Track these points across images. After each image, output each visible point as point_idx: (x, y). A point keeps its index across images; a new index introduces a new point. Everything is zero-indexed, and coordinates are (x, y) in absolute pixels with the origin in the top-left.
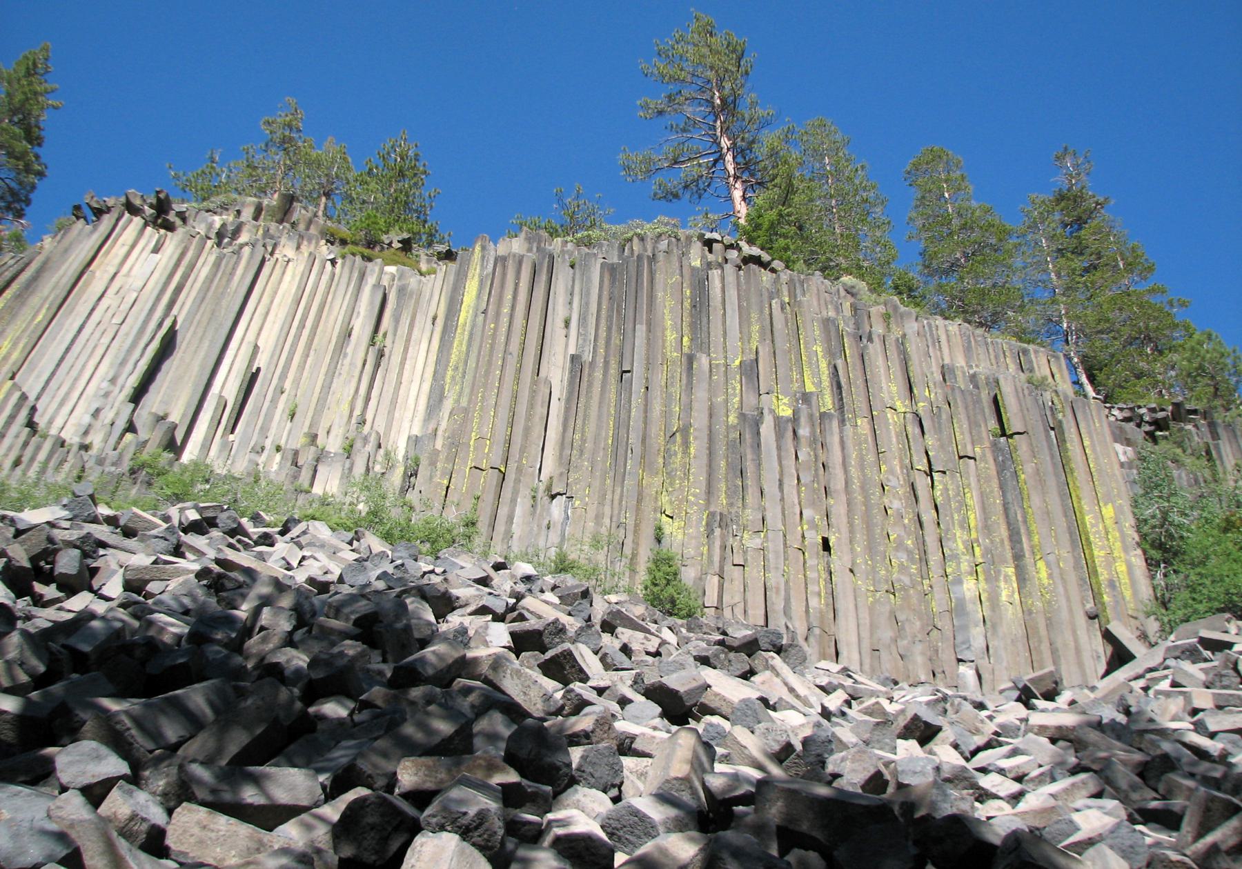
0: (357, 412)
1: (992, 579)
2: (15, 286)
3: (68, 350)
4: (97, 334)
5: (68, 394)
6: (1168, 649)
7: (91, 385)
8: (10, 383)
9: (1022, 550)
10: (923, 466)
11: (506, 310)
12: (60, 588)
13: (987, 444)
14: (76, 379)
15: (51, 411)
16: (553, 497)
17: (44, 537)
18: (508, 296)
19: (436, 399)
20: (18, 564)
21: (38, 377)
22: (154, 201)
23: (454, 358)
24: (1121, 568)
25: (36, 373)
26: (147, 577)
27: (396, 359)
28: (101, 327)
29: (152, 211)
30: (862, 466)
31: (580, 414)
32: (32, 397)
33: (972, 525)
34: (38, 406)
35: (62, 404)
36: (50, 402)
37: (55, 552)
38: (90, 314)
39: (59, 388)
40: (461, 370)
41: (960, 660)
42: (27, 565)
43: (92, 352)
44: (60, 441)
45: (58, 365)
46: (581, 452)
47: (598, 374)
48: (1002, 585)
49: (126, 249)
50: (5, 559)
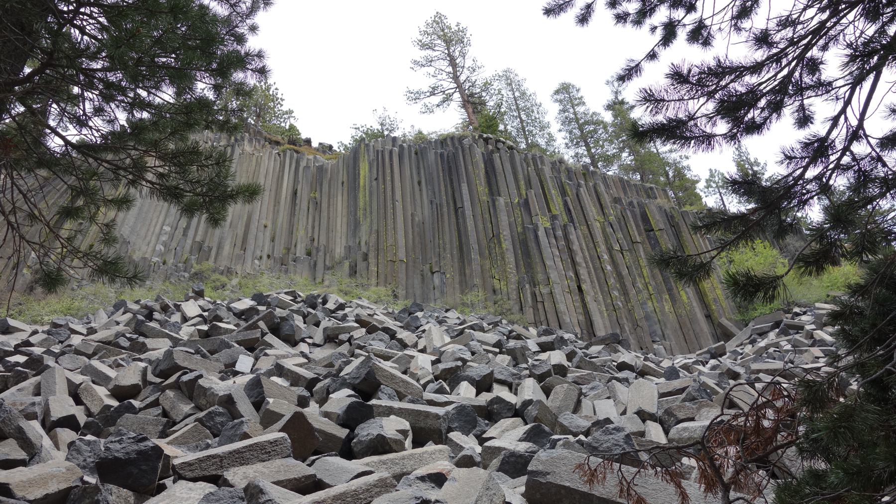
0: (310, 235)
1: (660, 301)
6: (753, 330)
9: (672, 286)
10: (617, 247)
11: (388, 178)
13: (645, 236)
16: (433, 273)
18: (388, 171)
19: (354, 226)
23: (361, 204)
24: (719, 292)
27: (324, 205)
30: (588, 250)
31: (440, 230)
33: (645, 275)
40: (368, 210)
41: (653, 341)
46: (444, 250)
47: (445, 209)
48: (665, 303)
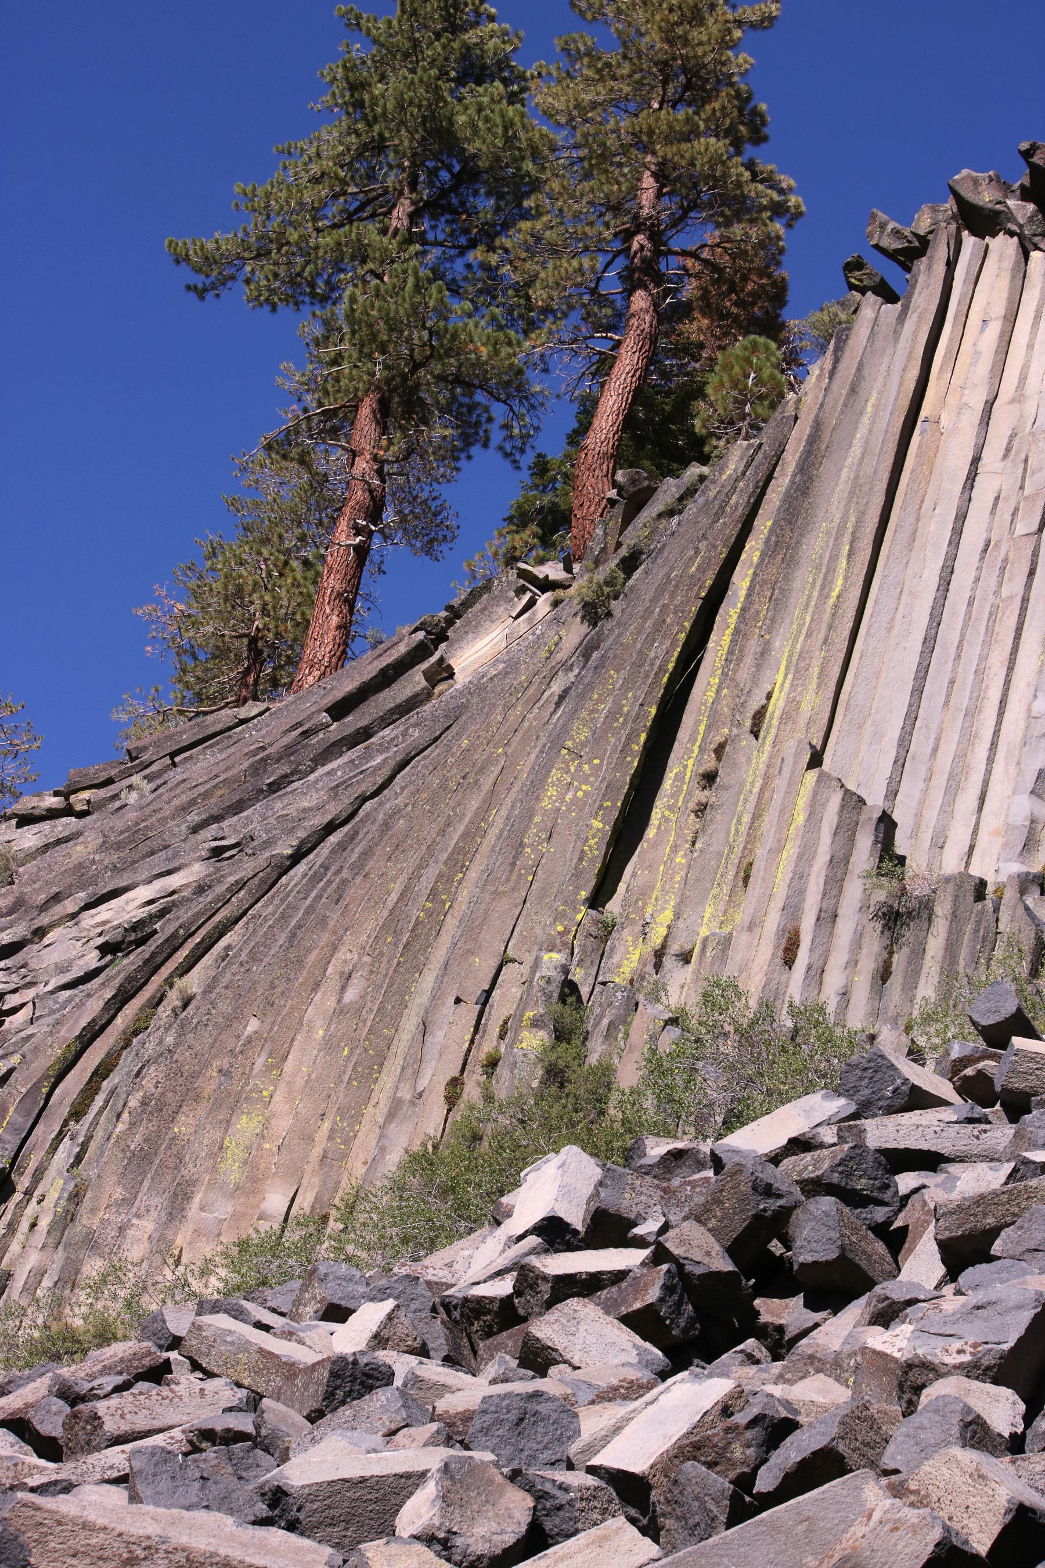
2: (763, 525)
3: (930, 643)
4: (990, 579)
5: (961, 756)
7: (1008, 716)
8: (813, 775)
12: (813, 1304)
14: (972, 713)
15: (931, 816)
17: (745, 1188)
20: (698, 1271)
21: (878, 736)
22: (1026, 181)
25: (869, 728)
26: (990, 1221)
28: (995, 558)
29: (1031, 207)
32: (875, 799)
34: (896, 817)
35: (953, 789)
36: (925, 792)
37: (784, 1215)
38: (958, 532)
39: (935, 750)
42: (726, 1265)
43: (990, 631)
44: (969, 888)
45: (918, 691)
49: (995, 329)
50: (665, 1267)
